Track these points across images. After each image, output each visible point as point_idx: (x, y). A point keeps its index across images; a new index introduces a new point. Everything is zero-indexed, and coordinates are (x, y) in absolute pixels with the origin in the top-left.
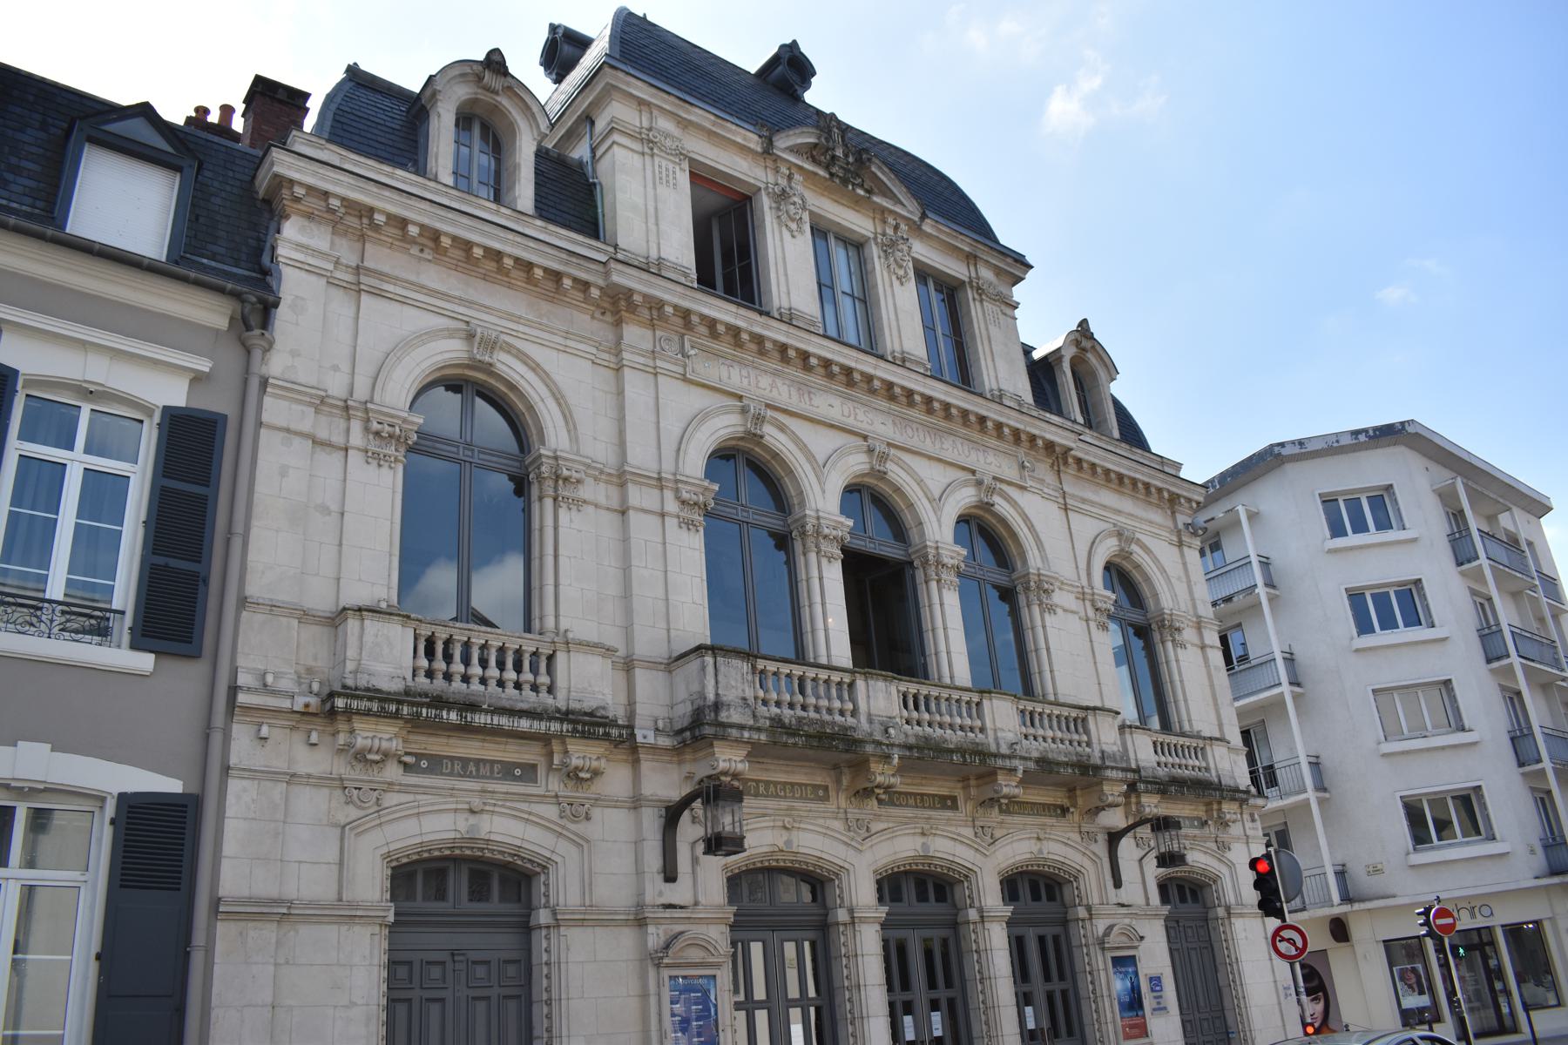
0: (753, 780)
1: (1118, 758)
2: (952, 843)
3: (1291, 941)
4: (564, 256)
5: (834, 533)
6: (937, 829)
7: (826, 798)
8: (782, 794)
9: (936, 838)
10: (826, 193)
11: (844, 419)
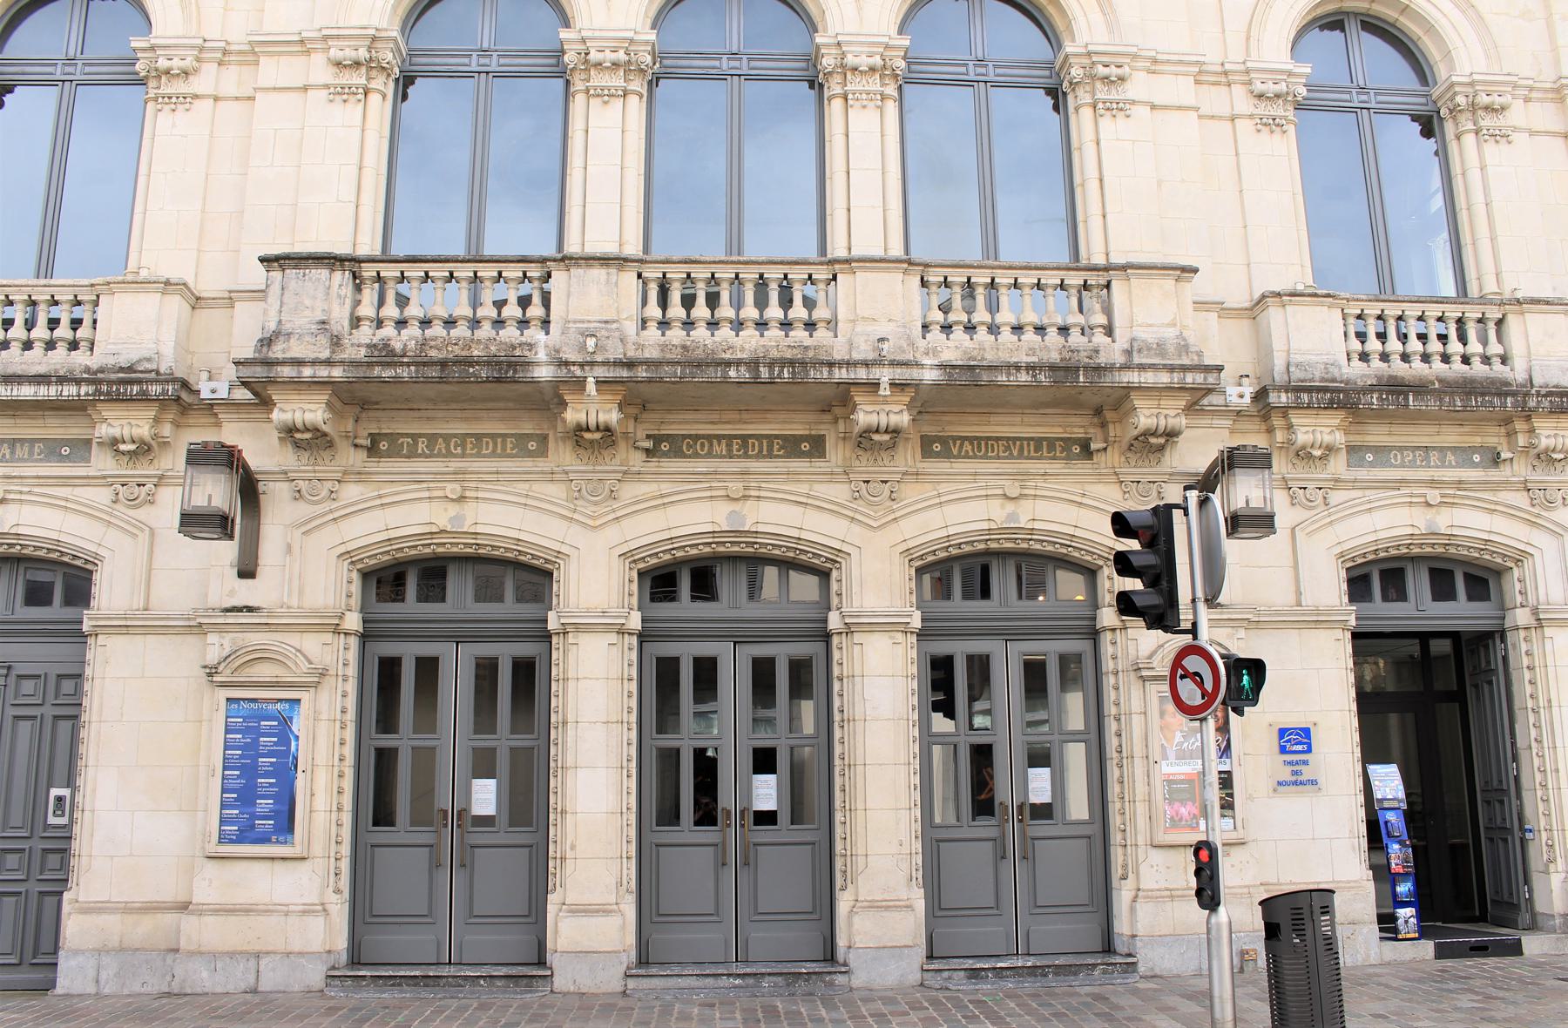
0: (407, 435)
1: (1171, 349)
2: (800, 509)
3: (1196, 677)
5: (613, 56)
6: (759, 489)
7: (542, 452)
8: (459, 450)
9: (763, 504)
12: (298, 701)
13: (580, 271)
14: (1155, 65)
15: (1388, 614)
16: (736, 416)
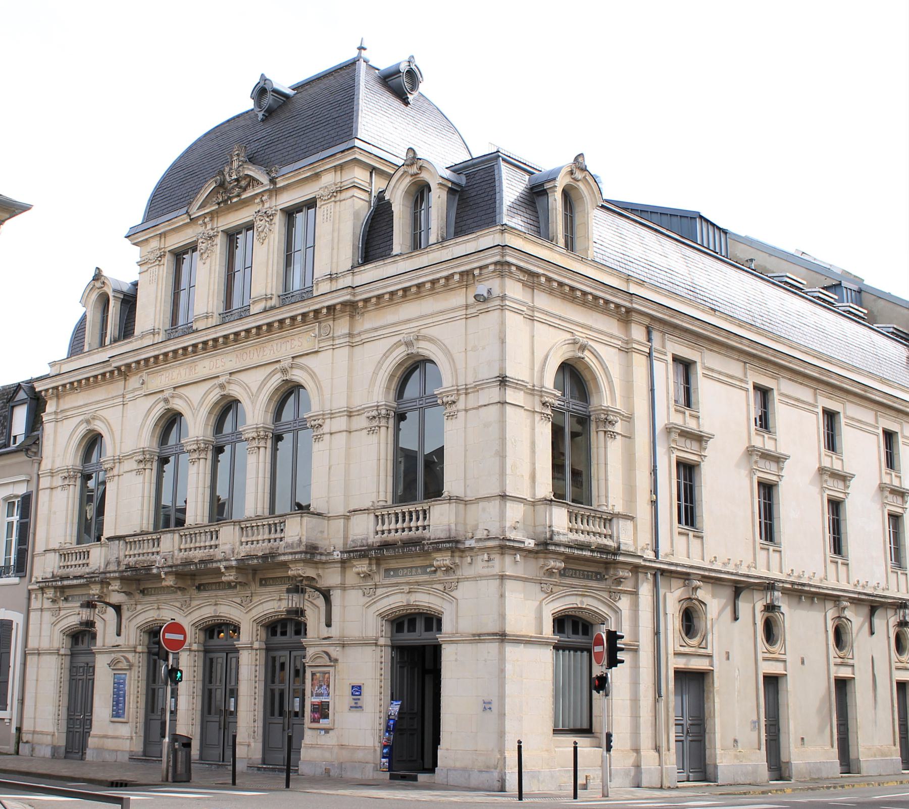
4: (102, 365)
10: (230, 211)
11: (210, 371)
12: (126, 674)
13: (165, 535)
14: (332, 416)
15: (409, 638)
16: (216, 576)
